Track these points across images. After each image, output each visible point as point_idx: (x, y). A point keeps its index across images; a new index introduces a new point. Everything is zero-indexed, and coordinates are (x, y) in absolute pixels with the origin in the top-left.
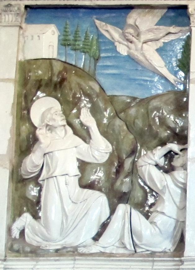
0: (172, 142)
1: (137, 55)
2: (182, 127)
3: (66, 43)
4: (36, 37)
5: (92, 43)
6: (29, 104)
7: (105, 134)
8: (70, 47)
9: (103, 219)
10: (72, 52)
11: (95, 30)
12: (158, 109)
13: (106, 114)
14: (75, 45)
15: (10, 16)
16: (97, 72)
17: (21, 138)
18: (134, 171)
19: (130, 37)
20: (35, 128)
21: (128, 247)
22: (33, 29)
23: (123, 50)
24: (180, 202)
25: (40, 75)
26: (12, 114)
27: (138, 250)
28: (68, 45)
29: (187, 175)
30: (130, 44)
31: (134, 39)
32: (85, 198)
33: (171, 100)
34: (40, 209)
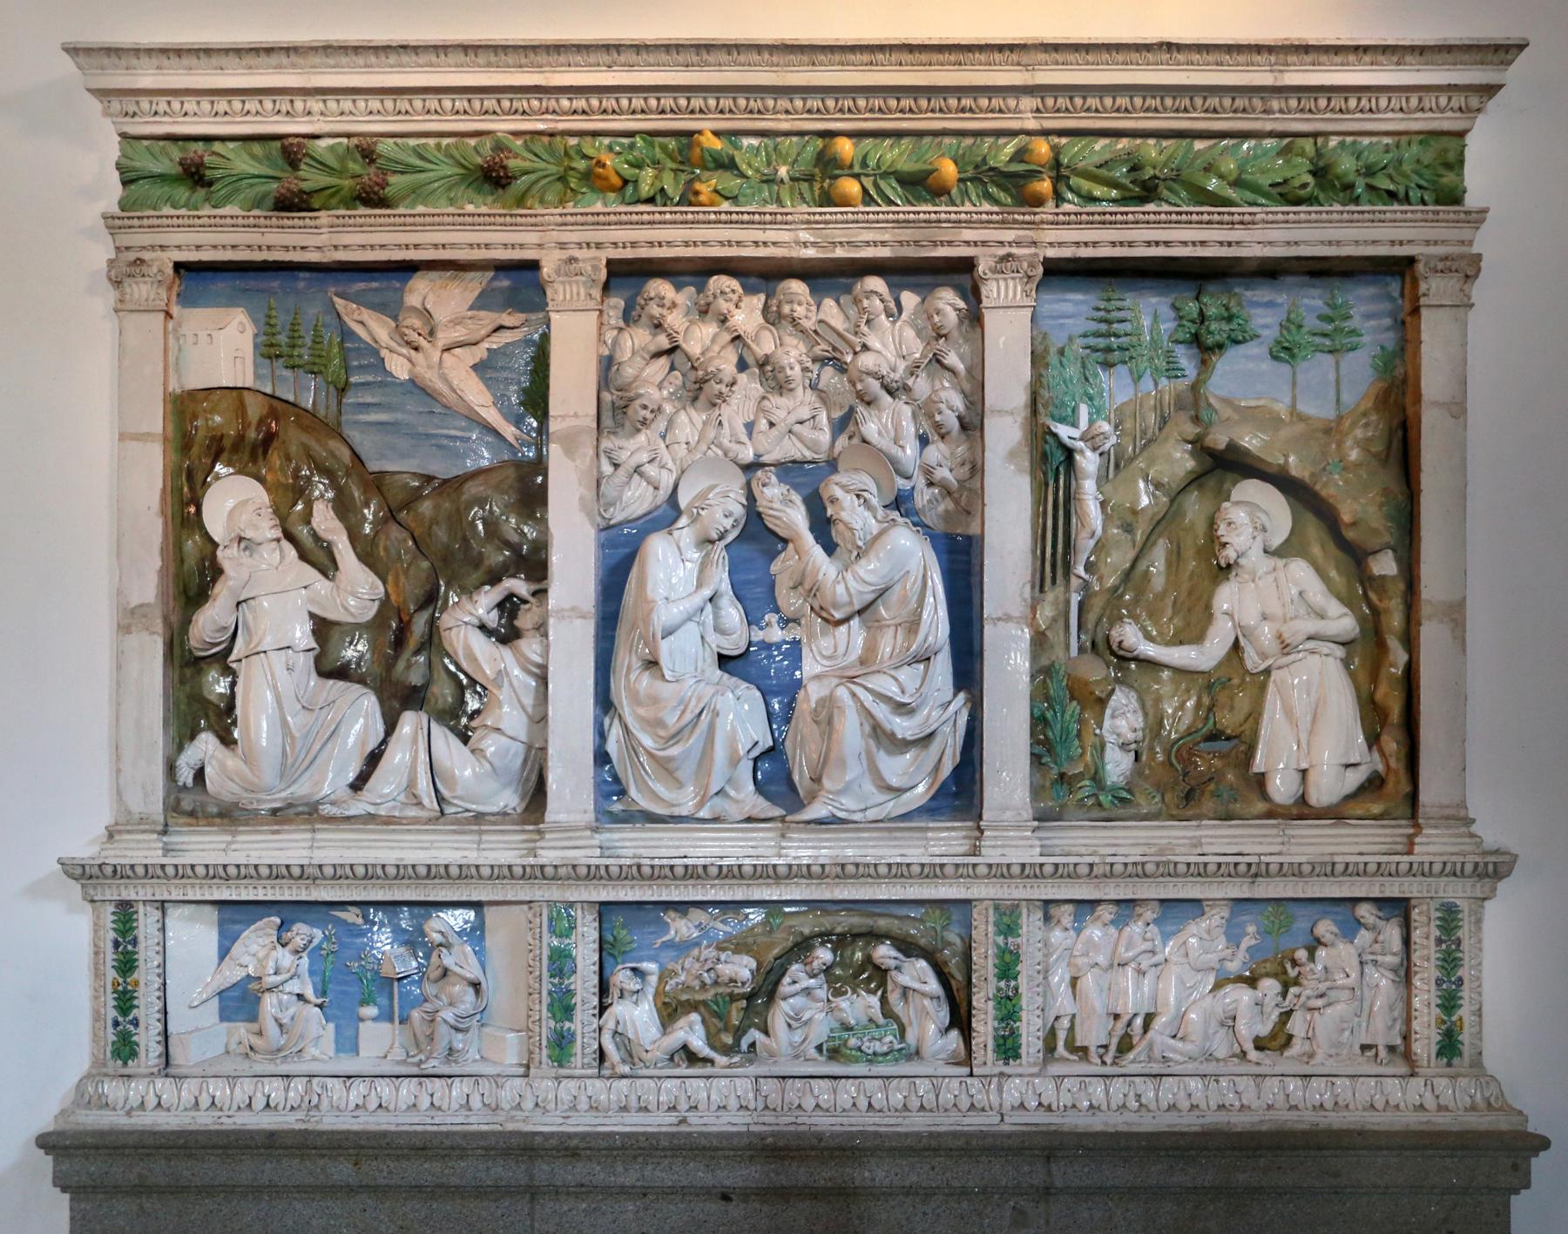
0: (514, 576)
1: (431, 378)
2: (534, 541)
3: (272, 350)
4: (203, 335)
5: (329, 352)
6: (200, 493)
7: (367, 557)
8: (281, 360)
9: (372, 744)
10: (288, 373)
11: (335, 322)
12: (481, 502)
13: (368, 513)
14: (291, 356)
15: (143, 286)
16: (344, 418)
17: (186, 567)
18: (432, 641)
19: (414, 336)
20: (215, 545)
21: (426, 802)
22: (196, 319)
23: (399, 367)
24: (534, 706)
25: (220, 426)
26: (163, 513)
27: (449, 810)
28: (278, 357)
29: (548, 646)
30: (413, 352)
31: (422, 342)
32: (331, 699)
33: (509, 481)
34: (234, 723)
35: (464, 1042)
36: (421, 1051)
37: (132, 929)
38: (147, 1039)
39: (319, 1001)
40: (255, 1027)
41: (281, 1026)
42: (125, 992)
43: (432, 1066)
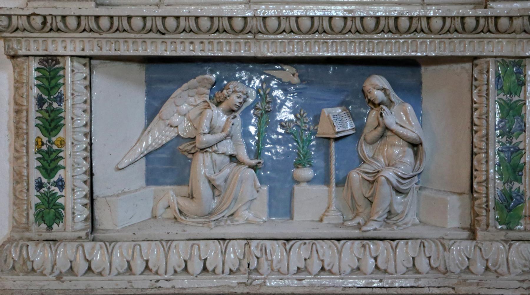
35: (405, 204)
36: (357, 215)
37: (58, 86)
38: (72, 200)
39: (254, 162)
40: (185, 190)
41: (214, 187)
42: (49, 152)
43: (372, 228)
